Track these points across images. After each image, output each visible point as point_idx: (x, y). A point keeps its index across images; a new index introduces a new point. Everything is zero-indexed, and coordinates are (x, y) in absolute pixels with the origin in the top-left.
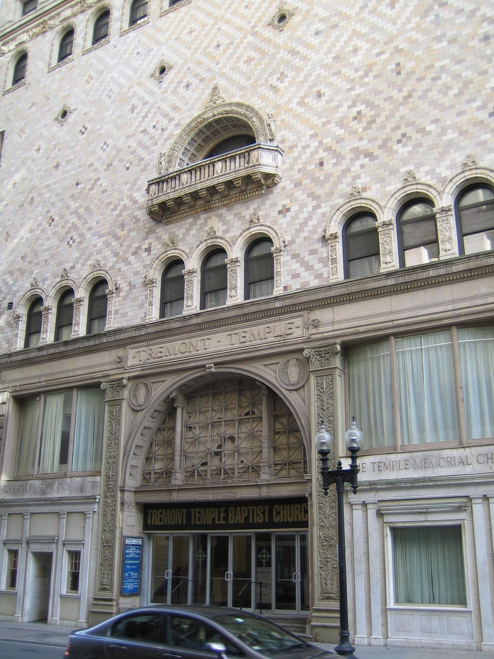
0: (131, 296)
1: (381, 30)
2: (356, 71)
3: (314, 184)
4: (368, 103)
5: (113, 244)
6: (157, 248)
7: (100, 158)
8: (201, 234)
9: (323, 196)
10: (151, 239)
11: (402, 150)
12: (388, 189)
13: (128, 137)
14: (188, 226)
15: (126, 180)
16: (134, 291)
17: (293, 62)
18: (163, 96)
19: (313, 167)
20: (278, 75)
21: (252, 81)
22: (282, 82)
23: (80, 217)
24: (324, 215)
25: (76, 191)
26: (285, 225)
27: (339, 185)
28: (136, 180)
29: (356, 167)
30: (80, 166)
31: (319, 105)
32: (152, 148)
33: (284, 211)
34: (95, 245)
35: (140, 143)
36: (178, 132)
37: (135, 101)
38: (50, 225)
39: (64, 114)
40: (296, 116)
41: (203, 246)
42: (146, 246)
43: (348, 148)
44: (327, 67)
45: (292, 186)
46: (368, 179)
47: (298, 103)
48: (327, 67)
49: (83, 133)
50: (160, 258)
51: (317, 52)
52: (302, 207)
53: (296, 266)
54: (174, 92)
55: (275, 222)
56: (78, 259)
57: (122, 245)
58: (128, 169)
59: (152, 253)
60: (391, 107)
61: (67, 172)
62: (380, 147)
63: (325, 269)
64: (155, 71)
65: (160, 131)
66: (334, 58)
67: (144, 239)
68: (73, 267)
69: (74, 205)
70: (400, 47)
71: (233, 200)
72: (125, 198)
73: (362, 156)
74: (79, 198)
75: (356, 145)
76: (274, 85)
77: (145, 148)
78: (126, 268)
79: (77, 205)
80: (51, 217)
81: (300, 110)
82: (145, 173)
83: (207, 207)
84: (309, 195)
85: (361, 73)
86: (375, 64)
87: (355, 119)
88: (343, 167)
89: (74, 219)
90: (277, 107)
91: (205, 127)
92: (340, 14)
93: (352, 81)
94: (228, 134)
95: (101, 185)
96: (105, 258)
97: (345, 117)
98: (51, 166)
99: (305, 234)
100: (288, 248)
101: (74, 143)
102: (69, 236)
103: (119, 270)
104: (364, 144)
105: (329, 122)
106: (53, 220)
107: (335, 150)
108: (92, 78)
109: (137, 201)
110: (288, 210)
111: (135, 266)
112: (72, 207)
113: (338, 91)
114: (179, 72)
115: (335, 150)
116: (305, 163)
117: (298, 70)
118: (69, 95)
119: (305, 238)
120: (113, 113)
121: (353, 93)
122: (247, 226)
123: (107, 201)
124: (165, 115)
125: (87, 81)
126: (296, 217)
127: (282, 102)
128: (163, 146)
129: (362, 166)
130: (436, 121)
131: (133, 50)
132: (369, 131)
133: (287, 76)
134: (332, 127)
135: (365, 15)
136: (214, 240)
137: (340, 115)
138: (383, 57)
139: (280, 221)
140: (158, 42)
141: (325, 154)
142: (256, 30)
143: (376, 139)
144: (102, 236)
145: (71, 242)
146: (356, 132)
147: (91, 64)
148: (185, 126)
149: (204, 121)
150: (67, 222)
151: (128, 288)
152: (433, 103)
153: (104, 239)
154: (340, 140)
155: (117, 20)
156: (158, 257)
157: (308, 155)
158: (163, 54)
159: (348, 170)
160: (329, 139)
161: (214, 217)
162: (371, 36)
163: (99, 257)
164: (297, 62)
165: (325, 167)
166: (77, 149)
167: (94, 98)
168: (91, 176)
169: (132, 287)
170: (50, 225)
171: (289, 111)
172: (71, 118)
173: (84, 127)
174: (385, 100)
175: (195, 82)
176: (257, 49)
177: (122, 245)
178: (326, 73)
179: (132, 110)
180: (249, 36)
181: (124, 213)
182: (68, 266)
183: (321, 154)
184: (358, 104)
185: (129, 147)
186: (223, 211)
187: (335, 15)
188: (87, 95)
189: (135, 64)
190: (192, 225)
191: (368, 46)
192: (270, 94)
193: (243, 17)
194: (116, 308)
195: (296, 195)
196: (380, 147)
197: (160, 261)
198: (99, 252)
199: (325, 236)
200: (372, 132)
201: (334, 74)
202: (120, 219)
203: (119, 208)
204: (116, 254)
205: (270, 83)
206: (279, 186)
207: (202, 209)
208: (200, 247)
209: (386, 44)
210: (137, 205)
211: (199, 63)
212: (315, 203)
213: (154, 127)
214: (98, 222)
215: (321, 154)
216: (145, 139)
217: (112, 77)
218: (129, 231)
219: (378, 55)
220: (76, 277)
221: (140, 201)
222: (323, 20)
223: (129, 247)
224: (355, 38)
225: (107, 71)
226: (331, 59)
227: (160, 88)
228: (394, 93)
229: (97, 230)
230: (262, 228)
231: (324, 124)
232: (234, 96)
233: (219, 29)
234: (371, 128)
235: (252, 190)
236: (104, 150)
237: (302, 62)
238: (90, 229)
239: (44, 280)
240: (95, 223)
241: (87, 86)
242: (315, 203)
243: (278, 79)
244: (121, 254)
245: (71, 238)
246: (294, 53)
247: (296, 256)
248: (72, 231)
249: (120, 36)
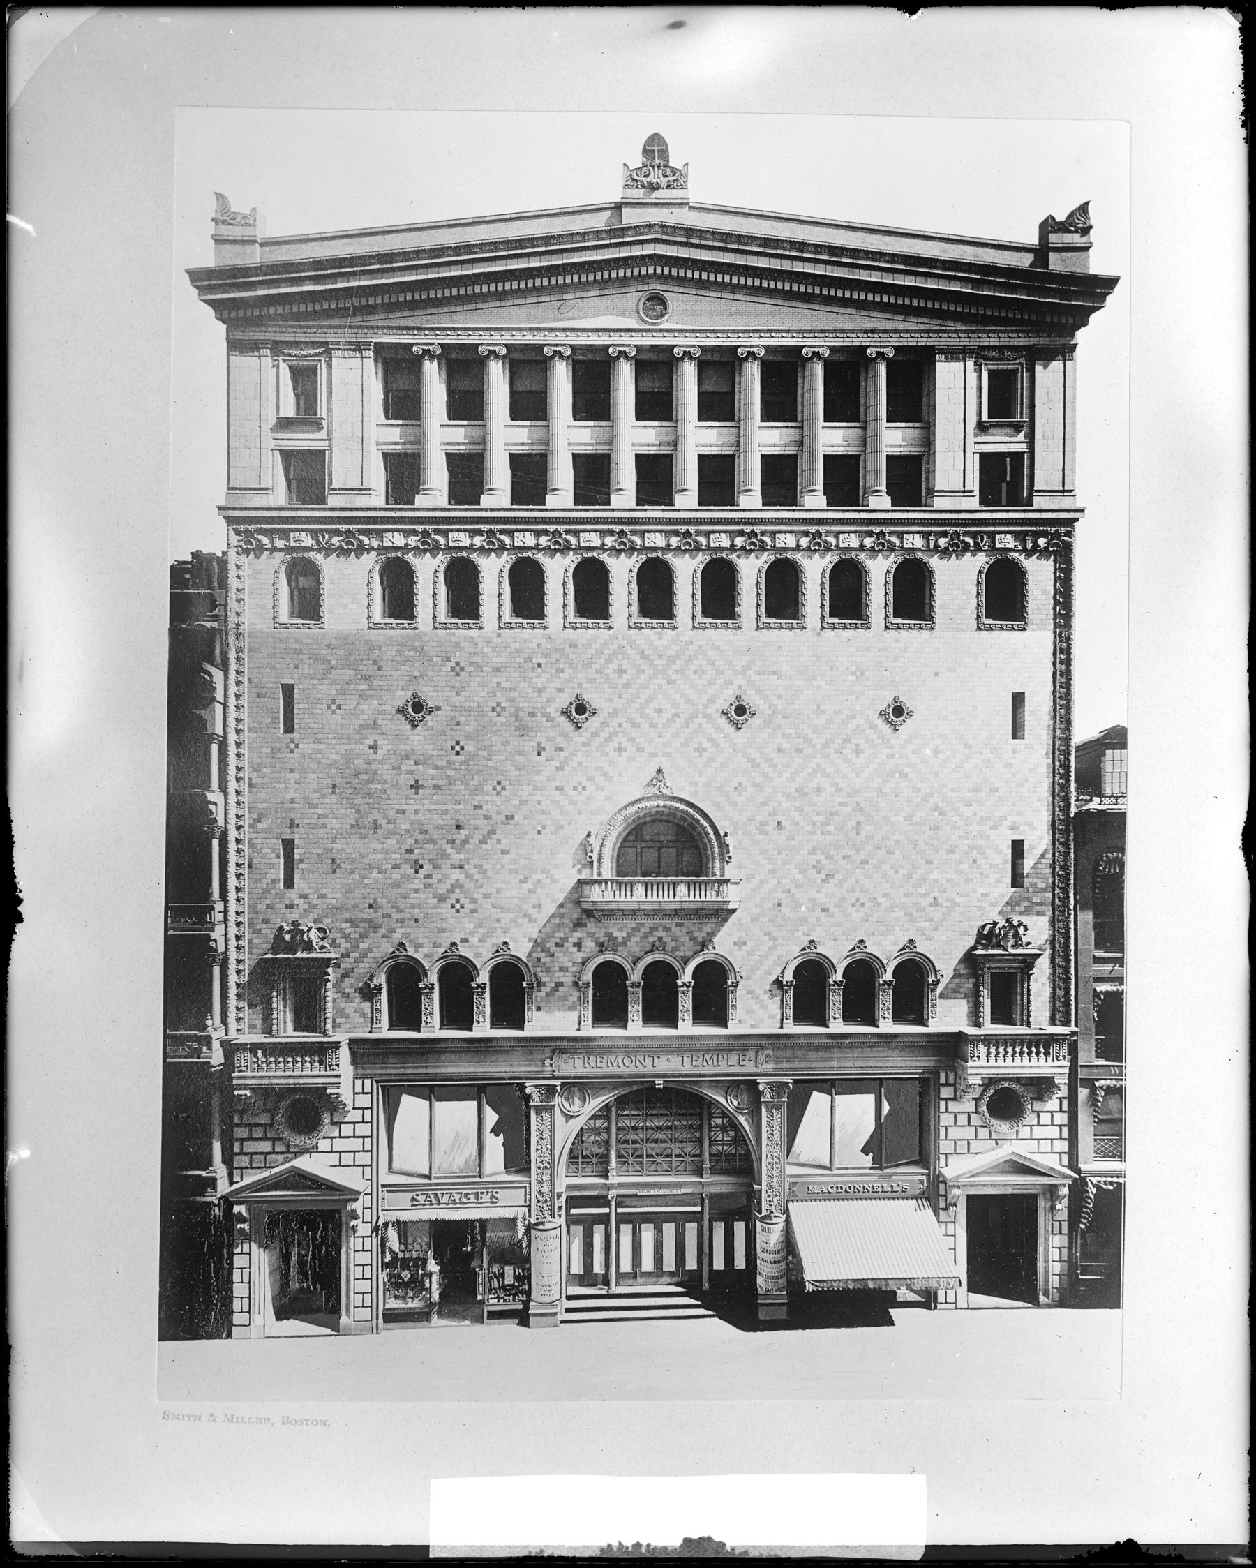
1: (845, 776)
11: (856, 915)
38: (417, 872)
44: (788, 796)
46: (823, 934)
48: (788, 796)
58: (539, 832)
80: (416, 861)
93: (814, 824)
102: (454, 896)
104: (821, 898)
106: (421, 867)
165: (783, 909)
170: (417, 872)
174: (844, 857)
200: (830, 887)
215: (779, 895)
219: (840, 804)
232: (683, 789)
238: (486, 896)
239: (418, 946)
245: (458, 901)
246: (755, 765)
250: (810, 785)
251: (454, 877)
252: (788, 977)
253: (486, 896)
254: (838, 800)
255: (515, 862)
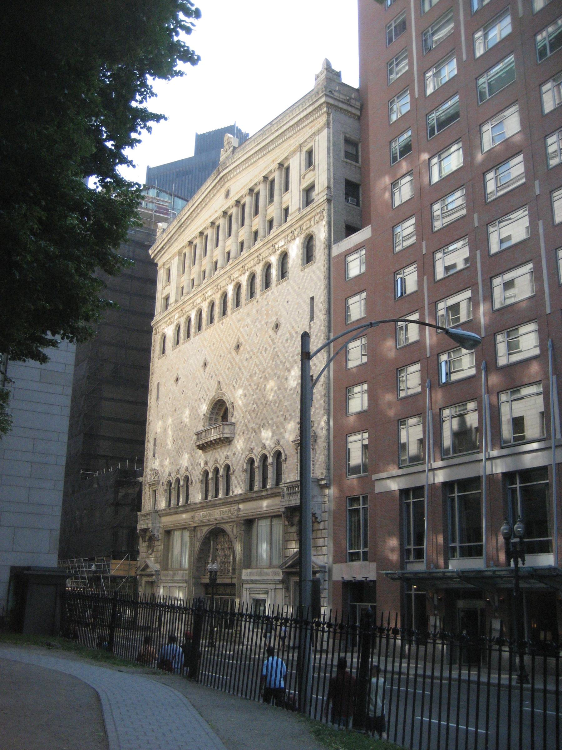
88: (248, 436)
94: (220, 410)
97: (250, 410)
98: (174, 409)
121: (254, 397)
130: (272, 419)
137: (249, 408)
152: (272, 409)
159: (250, 438)
176: (231, 362)
183: (244, 428)
186: (219, 450)
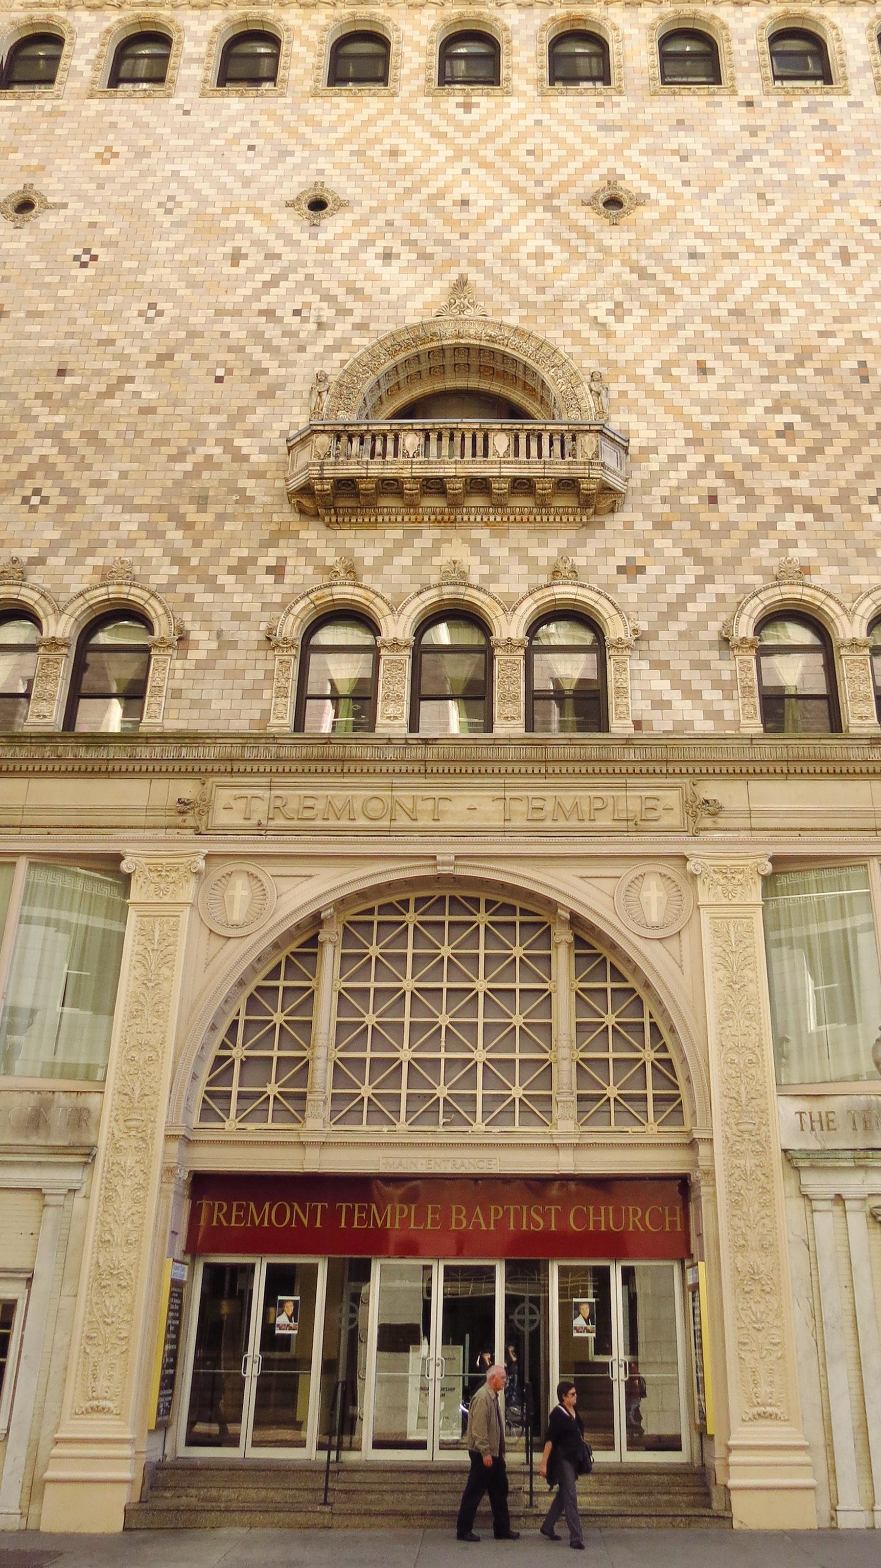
0: (221, 664)
1: (825, 292)
2: (779, 349)
3: (697, 533)
4: (805, 414)
5: (170, 535)
6: (301, 573)
7: (137, 335)
8: (425, 570)
9: (718, 562)
10: (285, 550)
12: (855, 580)
13: (220, 313)
14: (390, 545)
15: (214, 403)
16: (231, 654)
17: (643, 291)
18: (320, 257)
19: (695, 500)
20: (611, 306)
21: (548, 297)
22: (620, 319)
23: (65, 449)
24: (721, 597)
25: (57, 388)
26: (632, 598)
27: (752, 550)
28: (242, 412)
29: (788, 523)
30: (70, 335)
31: (703, 387)
32: (292, 356)
33: (631, 570)
34: (114, 526)
35: (257, 336)
36: (363, 341)
37: (242, 242)
39: (25, 206)
40: (651, 393)
41: (430, 597)
42: (273, 562)
43: (770, 484)
44: (716, 323)
45: (649, 525)
46: (812, 553)
47: (657, 371)
48: (716, 323)
49: (84, 265)
50: (312, 596)
51: (696, 291)
52: (673, 570)
53: (661, 685)
54: (352, 257)
55: (612, 587)
56: (54, 547)
57: (197, 544)
58: (219, 380)
59: (288, 579)
60: (854, 434)
61: (29, 337)
62: (834, 500)
63: (727, 705)
64: (298, 199)
65: (312, 326)
66: (731, 312)
67: (266, 545)
68: (40, 561)
69: (46, 418)
70: (865, 335)
71: (512, 518)
72: (211, 441)
73: (798, 508)
74: (64, 402)
75: (787, 483)
76: (600, 320)
77: (269, 348)
78: (209, 597)
79: (60, 419)
81: (660, 385)
82: (270, 402)
83: (446, 518)
84: (687, 552)
85: (790, 357)
86: (818, 349)
87: (780, 434)
89: (47, 448)
90: (611, 364)
91: (430, 353)
92: (740, 237)
93: (773, 364)
95: (137, 394)
96: (145, 561)
99: (682, 627)
100: (643, 646)
101: (56, 279)
102: (30, 485)
103: (189, 598)
104: (801, 486)
105: (726, 426)
107: (742, 482)
108: (116, 155)
109: (246, 458)
110: (641, 570)
111: (237, 598)
112: (42, 420)
113: (743, 374)
114: (363, 222)
115: (742, 482)
116: (679, 488)
117: (655, 309)
118: (42, 168)
119: (681, 634)
120: (179, 248)
122: (544, 580)
123: (157, 435)
124: (328, 298)
125: (99, 155)
126: (658, 587)
127: (621, 358)
128: (323, 359)
129: (801, 526)
131: (237, 138)
132: (811, 466)
133: (630, 312)
134: (733, 436)
135: (792, 255)
136: (462, 589)
138: (831, 342)
139: (621, 588)
140: (305, 144)
141: (720, 483)
142: (555, 202)
143: (826, 484)
144: (139, 509)
145: (35, 500)
146: (784, 459)
147: (113, 125)
148: (386, 334)
149: (432, 340)
150: (28, 451)
151: (214, 645)
153: (144, 517)
154: (751, 466)
155: (191, 60)
156: (308, 594)
157: (684, 475)
158: (321, 172)
160: (728, 458)
161: (457, 542)
162: (807, 298)
163: (128, 555)
164: (649, 292)
165: (722, 507)
166: (61, 293)
167: (121, 199)
168: (106, 365)
169: (226, 644)
171: (638, 380)
172: (47, 222)
173: (87, 251)
174: (841, 418)
175: (407, 255)
177: (197, 544)
178: (717, 334)
179: (236, 258)
180: (539, 209)
181: (205, 475)
182: (25, 554)
184: (786, 409)
185: (225, 334)
187: (730, 236)
188: (101, 187)
189: (248, 169)
190: (398, 547)
191: (802, 313)
192: (593, 335)
193: (524, 170)
194: (175, 684)
195: (658, 543)
196: (834, 500)
197: (312, 602)
198: (129, 543)
199: (727, 640)
200: (817, 468)
201: (734, 341)
202: (195, 484)
203: (191, 458)
204: (179, 560)
205: (592, 313)
206: (620, 518)
207: (433, 517)
208: (423, 597)
209: (836, 320)
210: (245, 466)
211: (416, 221)
212: (700, 570)
213: (297, 313)
214: (124, 475)
215: (711, 481)
216: (272, 332)
217: (175, 173)
218: (222, 518)
219: (822, 334)
220: (48, 586)
221: (253, 458)
222: (707, 237)
223: (220, 552)
224: (773, 291)
225: (163, 155)
226: (726, 313)
227: (314, 237)
228: (859, 411)
229: (120, 491)
230: (580, 591)
231: (714, 425)
232: (508, 312)
233: (466, 171)
234: (814, 461)
235: (561, 510)
236: (149, 321)
237: (662, 298)
240: (115, 475)
241: (100, 169)
242: (700, 570)
243: (609, 312)
244: (194, 562)
246: (643, 274)
247: (659, 665)
248: (40, 474)
249: (203, 95)
250: (759, 306)
251: (38, 452)
252: (745, 629)
253: (98, 484)
254: (815, 327)
255: (164, 425)
